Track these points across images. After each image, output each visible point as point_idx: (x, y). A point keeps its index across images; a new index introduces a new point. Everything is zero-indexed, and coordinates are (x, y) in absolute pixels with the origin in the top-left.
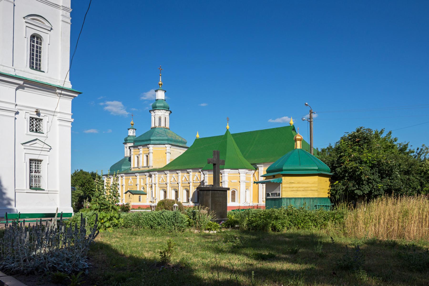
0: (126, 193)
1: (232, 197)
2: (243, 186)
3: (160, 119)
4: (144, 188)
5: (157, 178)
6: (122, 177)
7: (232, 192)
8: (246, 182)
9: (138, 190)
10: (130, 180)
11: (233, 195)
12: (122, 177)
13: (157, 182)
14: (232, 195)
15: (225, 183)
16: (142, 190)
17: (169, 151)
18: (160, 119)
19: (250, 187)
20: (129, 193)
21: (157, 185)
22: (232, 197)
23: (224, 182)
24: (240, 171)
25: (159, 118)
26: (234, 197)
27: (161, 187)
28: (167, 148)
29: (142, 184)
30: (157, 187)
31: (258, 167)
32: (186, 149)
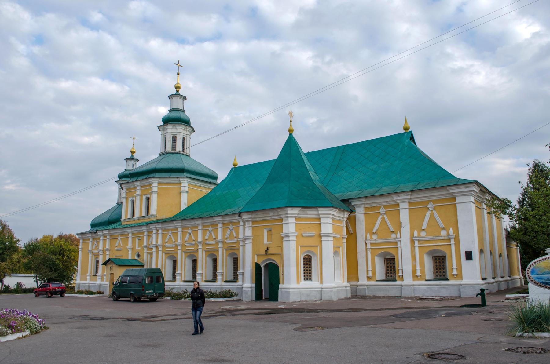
0: (105, 264)
1: (306, 269)
2: (328, 246)
3: (174, 139)
4: (139, 256)
5: (160, 236)
6: (105, 236)
7: (304, 259)
8: (333, 237)
9: (130, 257)
10: (118, 241)
11: (307, 264)
12: (105, 236)
13: (160, 242)
14: (304, 264)
15: (291, 238)
16: (136, 258)
17: (186, 189)
18: (174, 139)
19: (341, 248)
20: (110, 265)
21: (160, 249)
22: (306, 269)
23: (288, 236)
24: (322, 212)
25: (173, 137)
26: (309, 269)
27: (170, 252)
28: (183, 185)
29: (137, 248)
30: (160, 253)
31: (353, 206)
32: (215, 186)
